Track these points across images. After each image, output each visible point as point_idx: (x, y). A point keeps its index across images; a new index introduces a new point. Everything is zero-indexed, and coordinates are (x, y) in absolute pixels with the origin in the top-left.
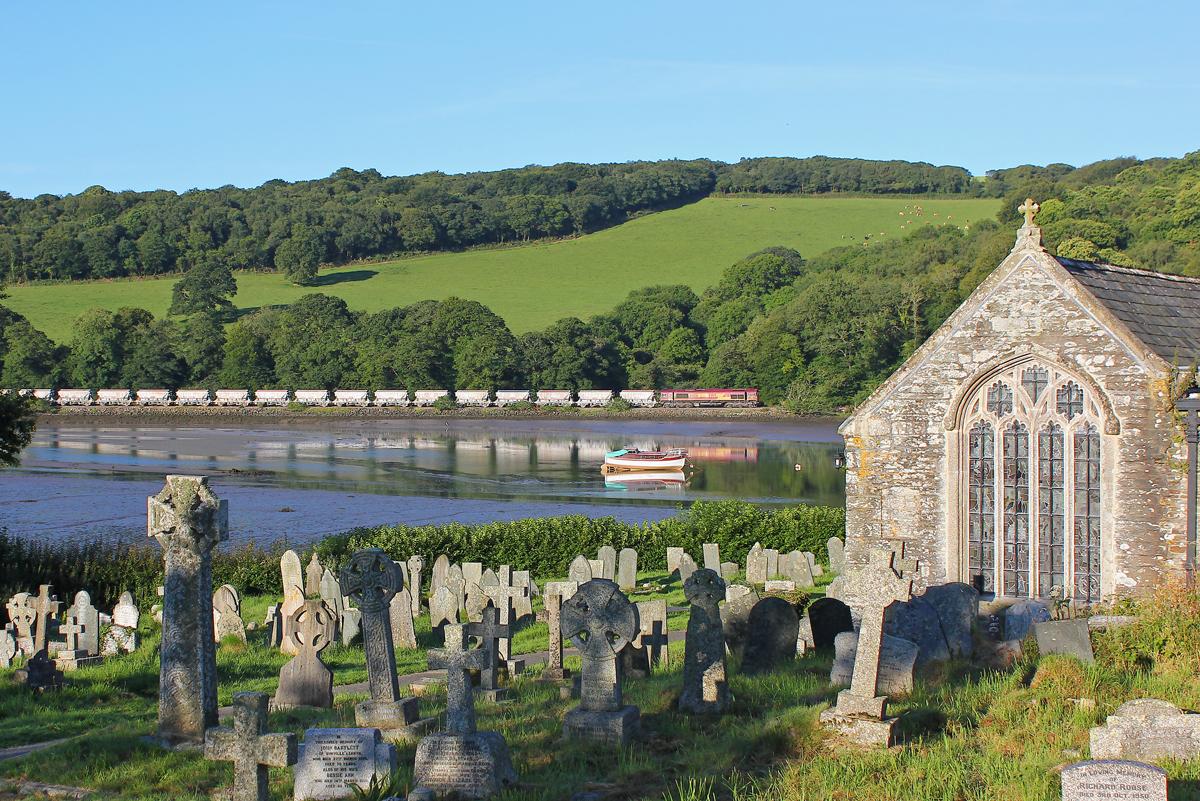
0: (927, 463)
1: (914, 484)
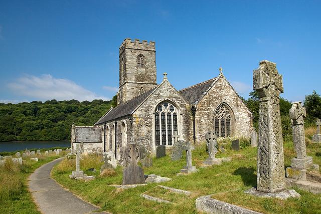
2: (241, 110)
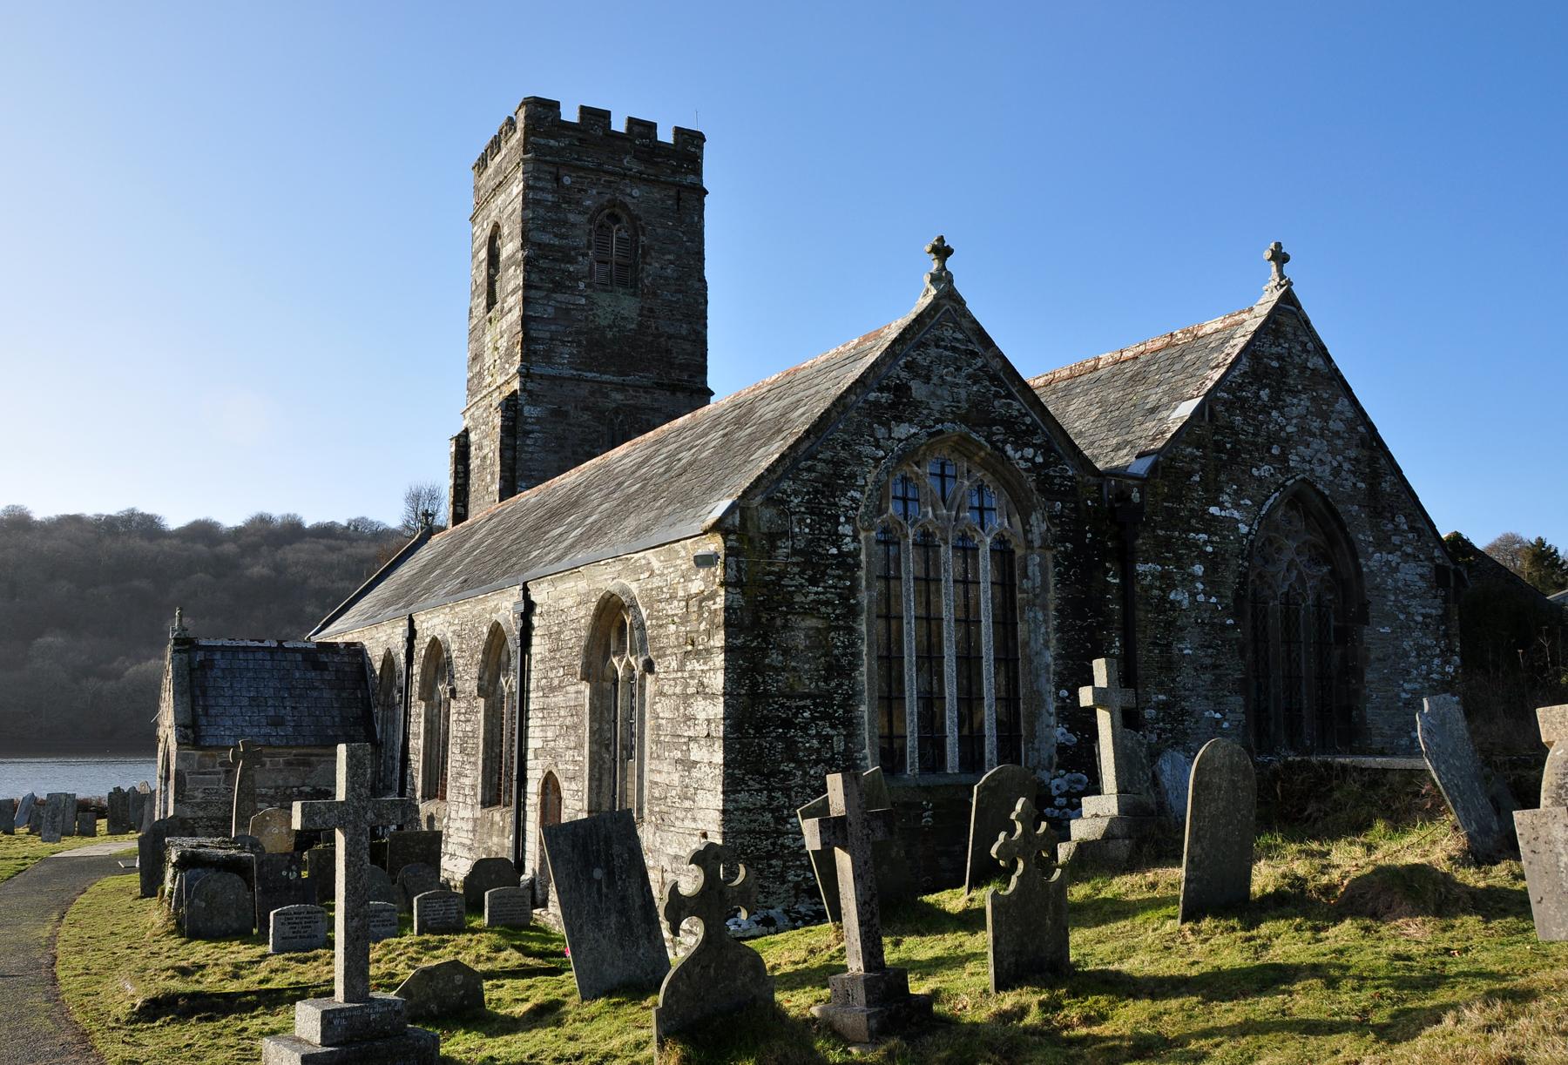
0: (840, 578)
1: (823, 609)
2: (1396, 540)
